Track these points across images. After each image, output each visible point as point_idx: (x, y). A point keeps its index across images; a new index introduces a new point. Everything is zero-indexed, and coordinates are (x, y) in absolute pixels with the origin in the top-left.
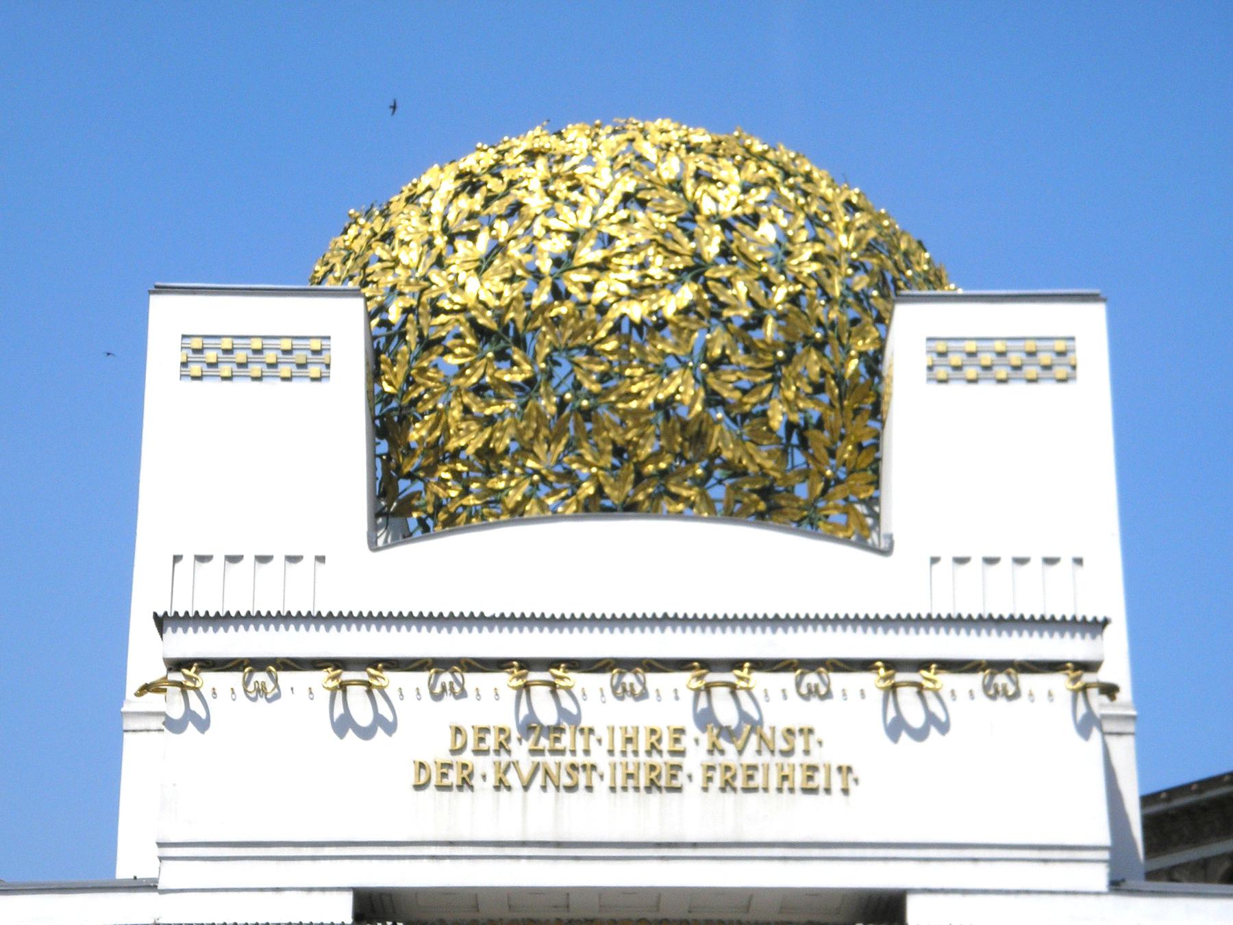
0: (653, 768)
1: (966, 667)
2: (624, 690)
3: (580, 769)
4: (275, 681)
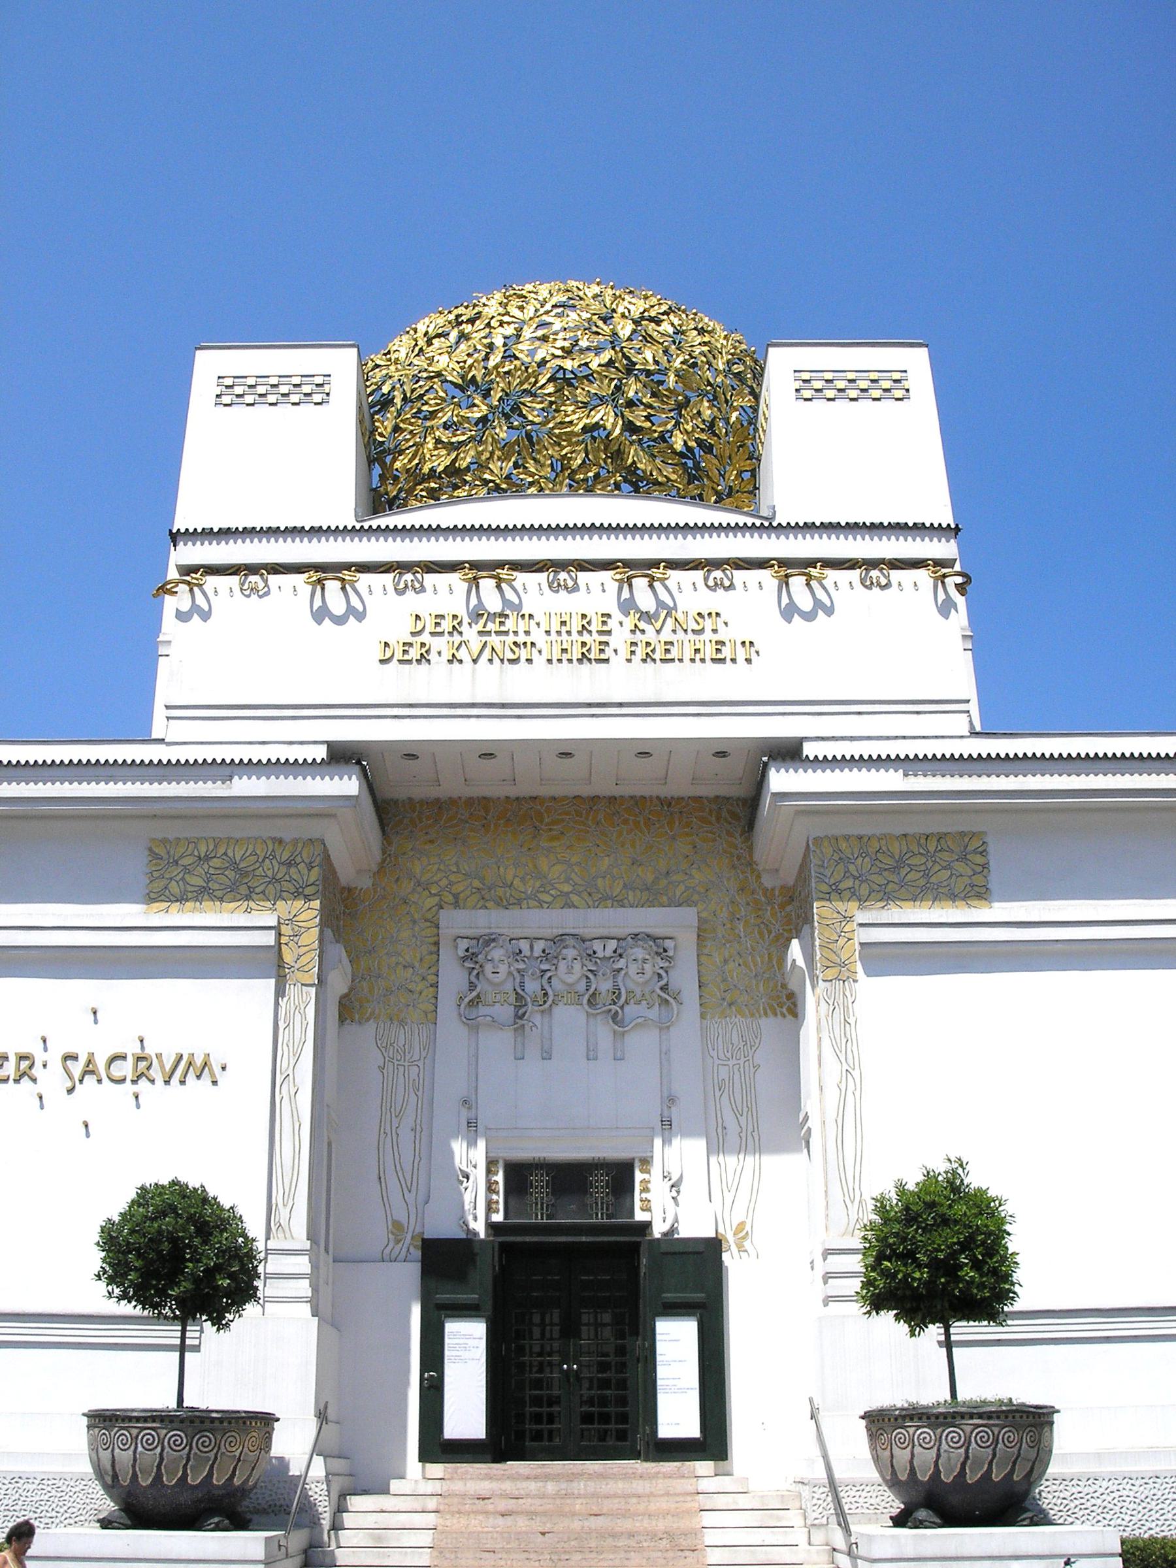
0: (584, 644)
1: (846, 565)
2: (559, 585)
3: (522, 646)
4: (266, 581)
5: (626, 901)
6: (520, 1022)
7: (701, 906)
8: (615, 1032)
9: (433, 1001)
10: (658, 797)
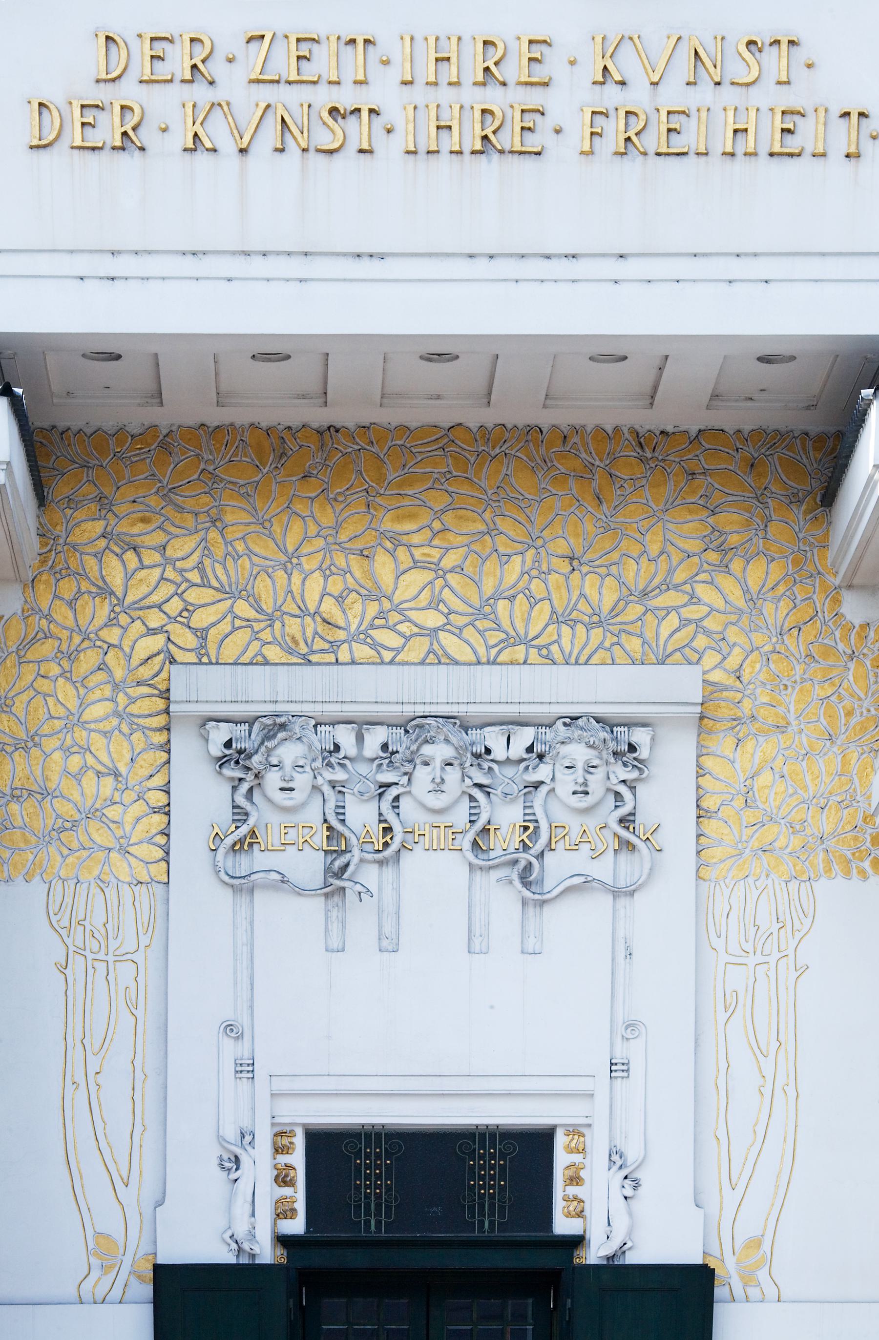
5: (555, 648)
6: (338, 883)
7: (711, 659)
8: (524, 902)
9: (162, 840)
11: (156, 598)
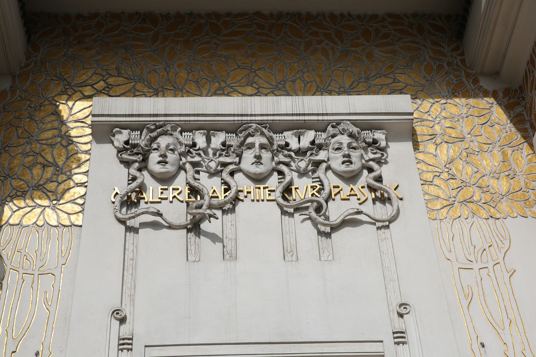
9: (81, 201)
10: (349, 14)
11: (90, 82)
